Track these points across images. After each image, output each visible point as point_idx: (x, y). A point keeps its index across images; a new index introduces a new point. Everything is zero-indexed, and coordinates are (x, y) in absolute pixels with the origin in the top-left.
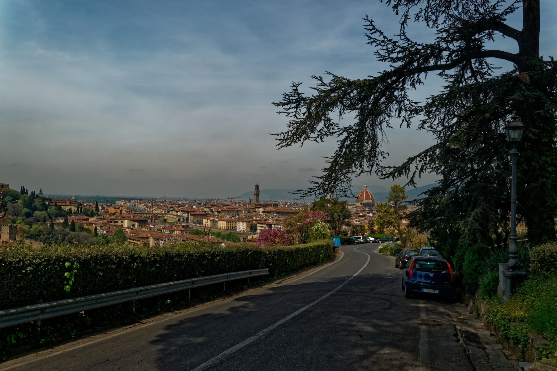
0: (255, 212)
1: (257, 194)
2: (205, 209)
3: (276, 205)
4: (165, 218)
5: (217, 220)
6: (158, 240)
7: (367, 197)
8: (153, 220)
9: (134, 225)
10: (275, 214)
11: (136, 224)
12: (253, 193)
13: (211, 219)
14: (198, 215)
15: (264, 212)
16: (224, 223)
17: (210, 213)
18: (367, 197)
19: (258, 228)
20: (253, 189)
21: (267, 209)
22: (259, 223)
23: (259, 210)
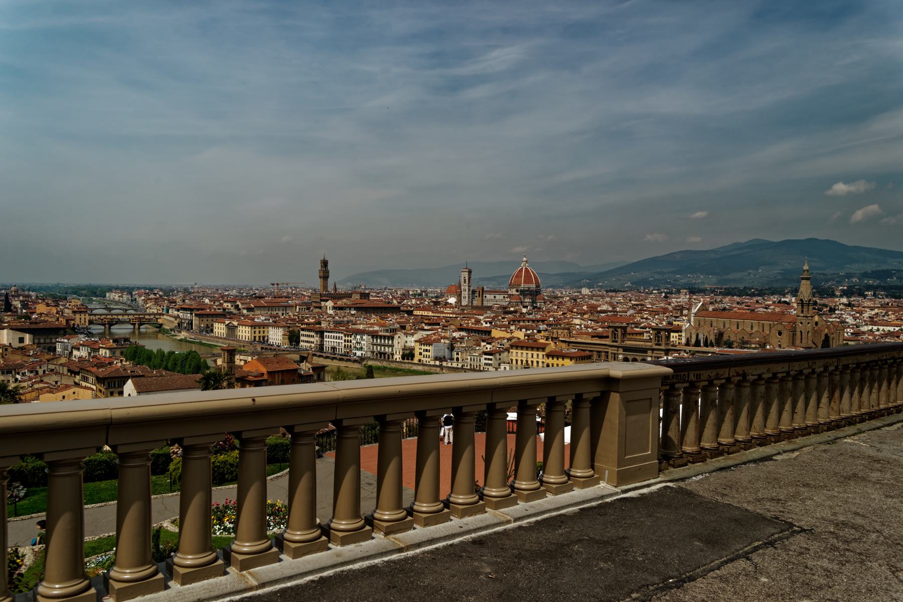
0: (320, 308)
1: (325, 276)
2: (225, 305)
3: (365, 296)
4: (160, 321)
5: (235, 323)
6: (9, 372)
7: (528, 279)
8: (137, 326)
9: (21, 340)
10: (353, 312)
11: (28, 338)
12: (317, 274)
13: (227, 322)
14: (208, 315)
15: (334, 308)
16: (248, 329)
17: (235, 311)
18: (528, 279)
19: (302, 338)
20: (319, 266)
21: (339, 303)
22: (303, 330)
23: (327, 304)
